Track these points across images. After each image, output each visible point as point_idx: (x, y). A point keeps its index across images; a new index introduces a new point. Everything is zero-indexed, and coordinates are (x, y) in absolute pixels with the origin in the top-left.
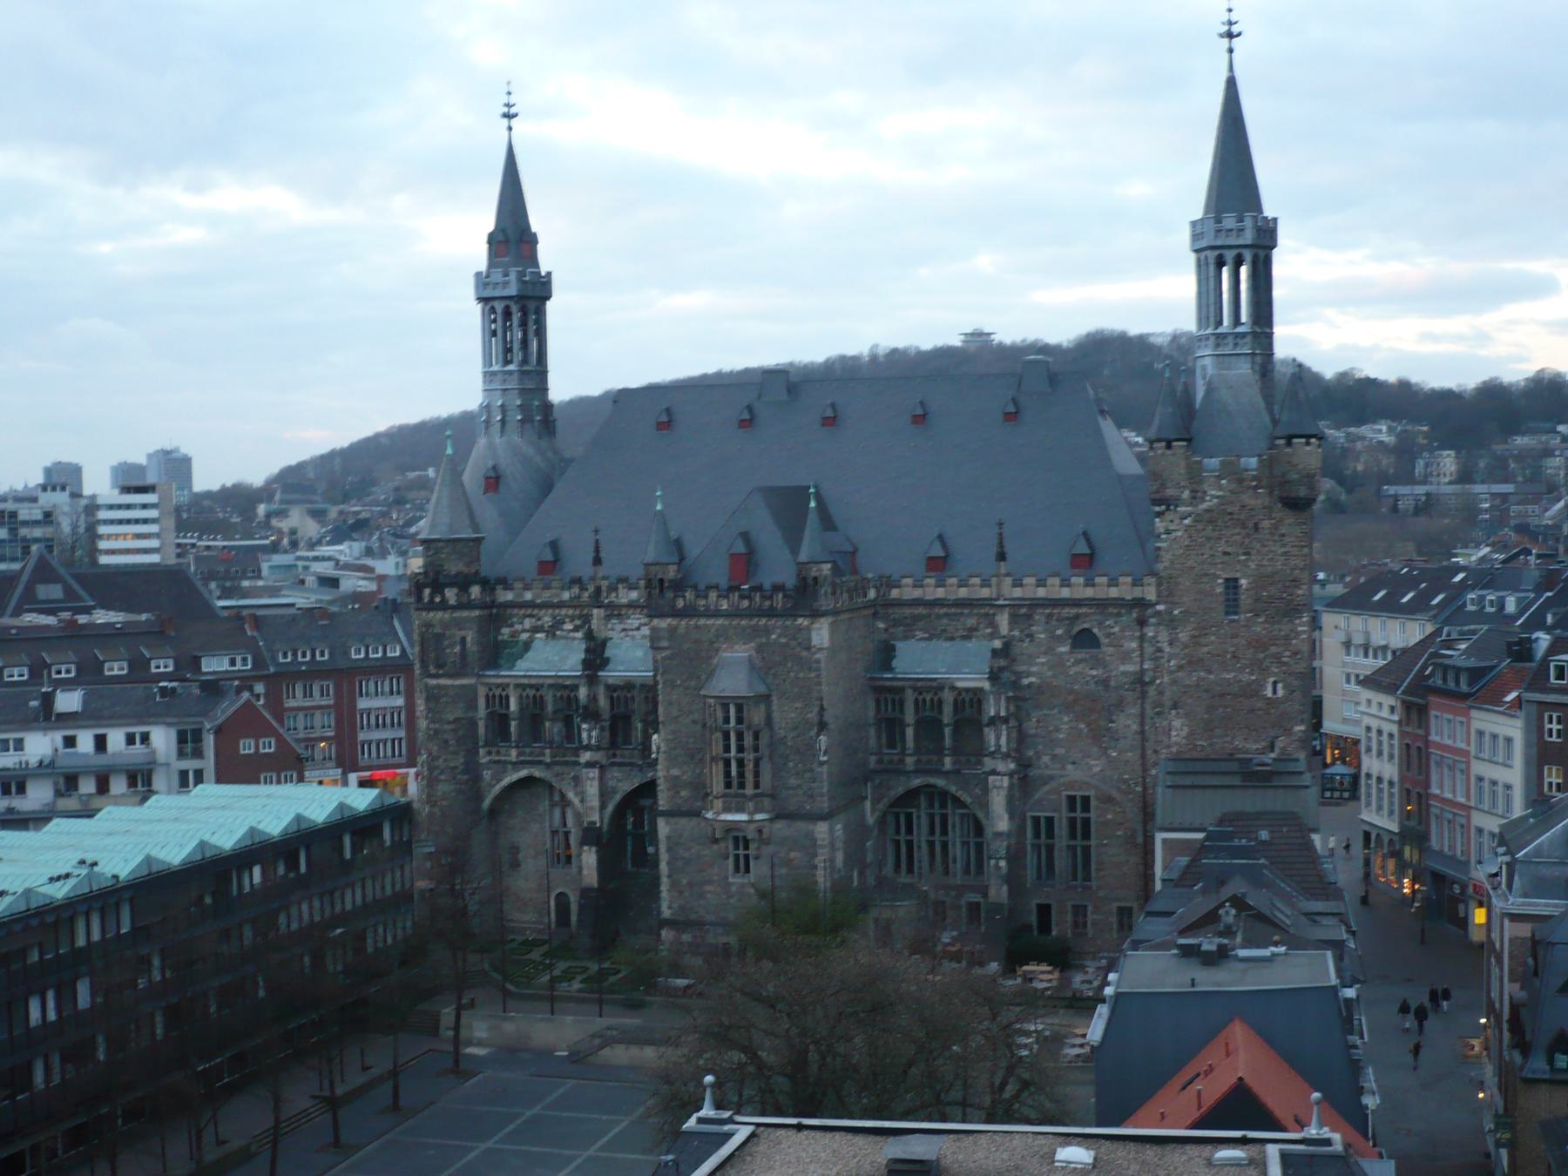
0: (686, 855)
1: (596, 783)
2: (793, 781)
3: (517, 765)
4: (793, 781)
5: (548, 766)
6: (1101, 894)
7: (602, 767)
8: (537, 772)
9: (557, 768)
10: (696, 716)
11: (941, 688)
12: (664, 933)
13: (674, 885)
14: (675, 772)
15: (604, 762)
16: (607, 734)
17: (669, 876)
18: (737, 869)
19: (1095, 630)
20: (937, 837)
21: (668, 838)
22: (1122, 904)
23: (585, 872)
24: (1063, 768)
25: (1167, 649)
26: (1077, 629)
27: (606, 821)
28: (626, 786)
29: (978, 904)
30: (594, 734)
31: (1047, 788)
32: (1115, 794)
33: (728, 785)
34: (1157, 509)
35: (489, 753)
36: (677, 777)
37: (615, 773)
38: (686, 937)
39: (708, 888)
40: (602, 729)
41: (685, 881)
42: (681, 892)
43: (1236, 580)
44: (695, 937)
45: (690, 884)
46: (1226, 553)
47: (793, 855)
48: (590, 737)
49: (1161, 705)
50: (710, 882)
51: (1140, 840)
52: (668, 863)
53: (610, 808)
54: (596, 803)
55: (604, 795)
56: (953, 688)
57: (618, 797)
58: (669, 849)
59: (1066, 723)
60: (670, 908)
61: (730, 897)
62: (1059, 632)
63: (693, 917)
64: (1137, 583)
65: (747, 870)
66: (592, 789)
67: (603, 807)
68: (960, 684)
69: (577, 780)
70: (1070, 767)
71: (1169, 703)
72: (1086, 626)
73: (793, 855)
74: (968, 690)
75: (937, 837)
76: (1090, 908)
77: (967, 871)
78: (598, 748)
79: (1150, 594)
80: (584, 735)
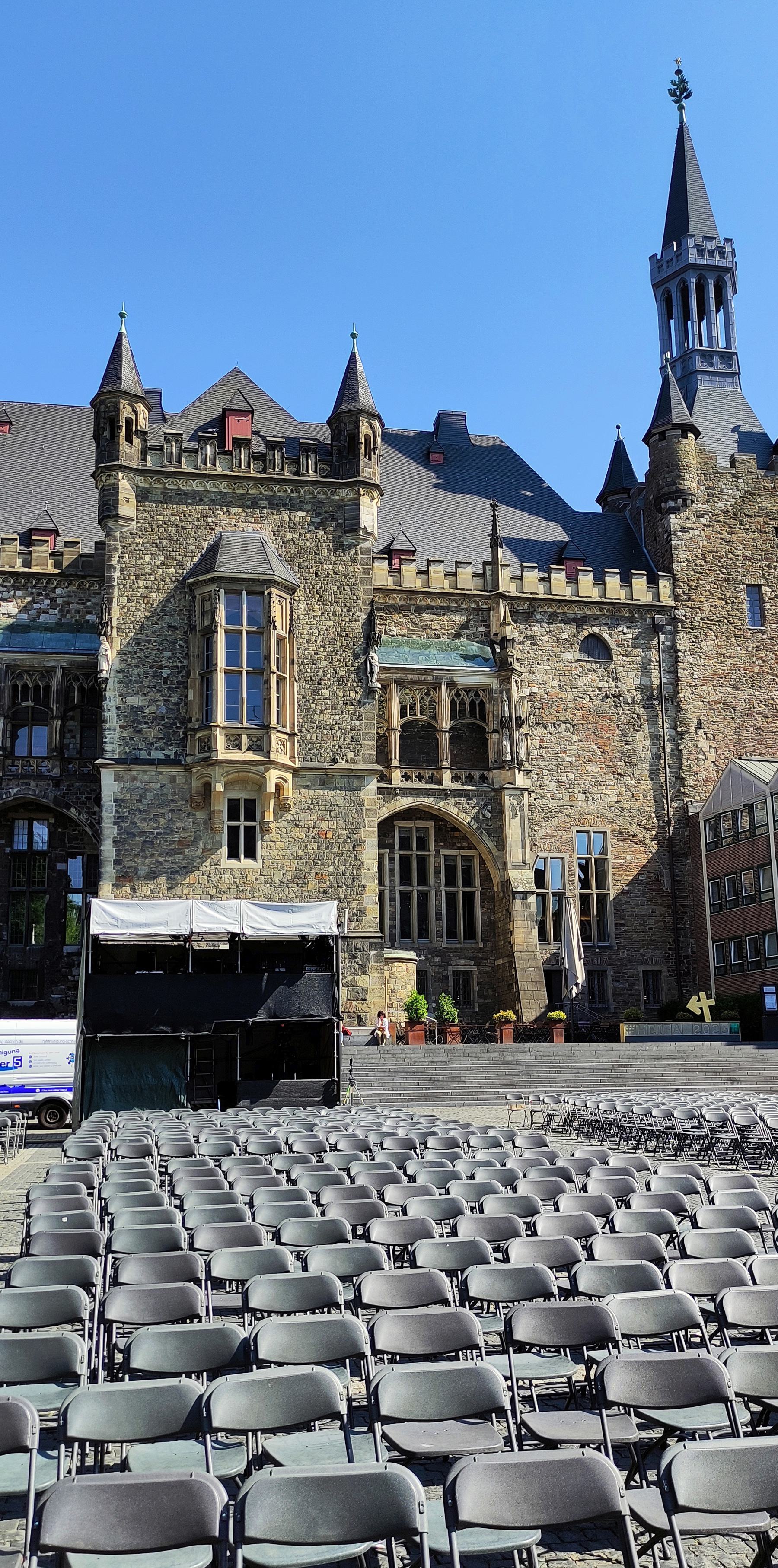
2: (328, 718)
4: (328, 718)
6: (623, 955)
10: (176, 621)
11: (436, 685)
14: (136, 701)
17: (117, 863)
18: (233, 854)
19: (606, 636)
20: (415, 890)
22: (650, 968)
24: (572, 797)
25: (689, 658)
26: (585, 633)
29: (468, 974)
31: (554, 822)
32: (633, 828)
33: (232, 713)
34: (671, 504)
36: (141, 708)
43: (759, 586)
46: (746, 558)
47: (325, 825)
49: (685, 723)
51: (666, 886)
56: (451, 685)
59: (572, 743)
62: (565, 636)
64: (653, 581)
65: (251, 853)
68: (458, 679)
70: (581, 797)
71: (694, 723)
72: (596, 630)
73: (325, 825)
74: (467, 691)
75: (415, 890)
76: (610, 973)
77: (452, 934)
79: (666, 600)
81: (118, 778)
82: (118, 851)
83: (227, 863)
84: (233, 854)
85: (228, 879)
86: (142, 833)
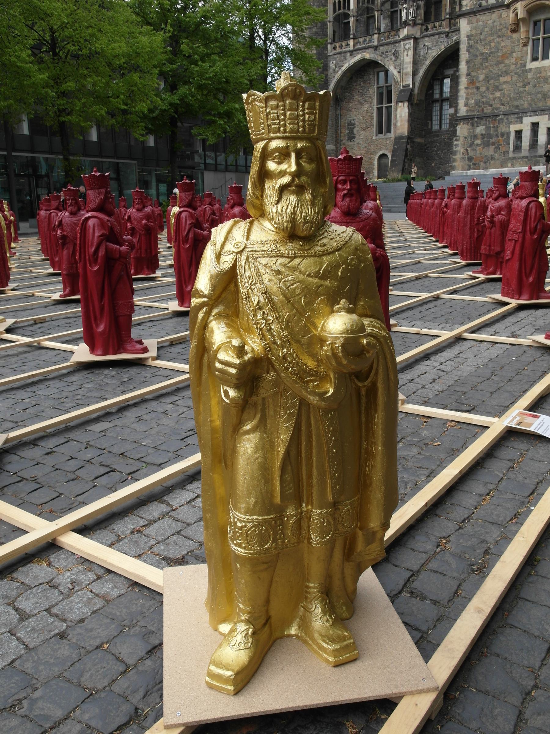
0: (486, 50)
1: (411, 53)
3: (352, 53)
5: (376, 48)
7: (416, 39)
8: (368, 55)
9: (381, 48)
12: (458, 128)
13: (472, 82)
15: (418, 35)
16: (422, 11)
17: (468, 75)
21: (469, 37)
23: (399, 124)
27: (417, 84)
28: (434, 53)
30: (411, 11)
35: (335, 48)
37: (427, 42)
38: (480, 129)
39: (502, 79)
40: (418, 8)
41: (482, 77)
42: (478, 88)
44: (488, 128)
45: (487, 79)
48: (408, 14)
50: (506, 73)
52: (467, 62)
53: (421, 73)
54: (409, 69)
55: (416, 63)
57: (428, 63)
58: (470, 48)
60: (466, 105)
61: (524, 86)
63: (488, 110)
66: (408, 59)
67: (415, 73)
69: (396, 54)
78: (415, 24)
80: (404, 13)
81: (469, 23)
82: (468, 68)
83: (532, 65)
84: (535, 59)
85: (530, 75)
86: (482, 54)
